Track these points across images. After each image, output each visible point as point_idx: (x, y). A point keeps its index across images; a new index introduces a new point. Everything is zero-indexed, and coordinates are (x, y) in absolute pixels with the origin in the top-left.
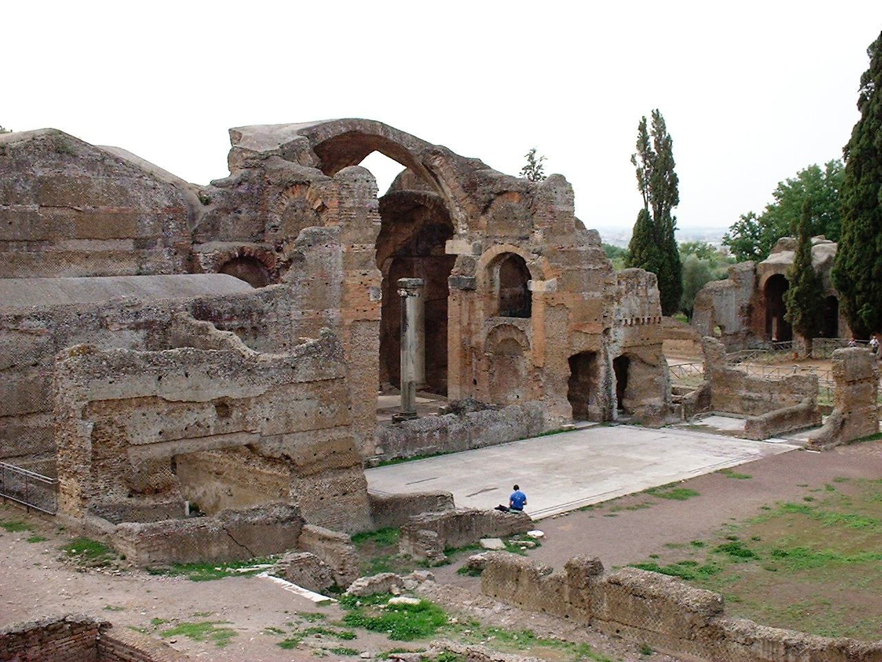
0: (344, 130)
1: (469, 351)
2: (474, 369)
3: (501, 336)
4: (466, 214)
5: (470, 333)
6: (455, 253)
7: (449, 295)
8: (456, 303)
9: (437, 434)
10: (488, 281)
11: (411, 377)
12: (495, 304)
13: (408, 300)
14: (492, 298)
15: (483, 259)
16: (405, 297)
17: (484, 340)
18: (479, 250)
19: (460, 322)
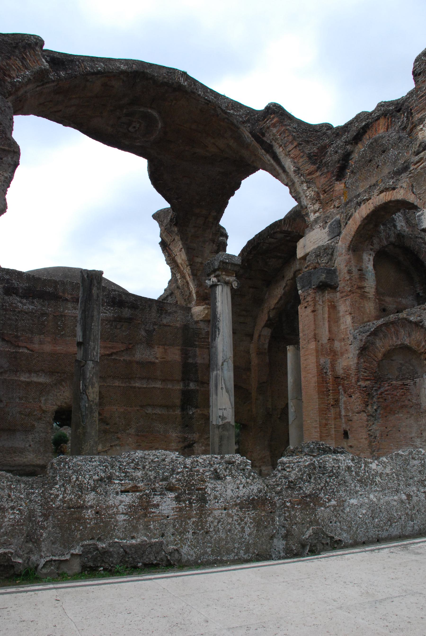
0: (123, 67)
1: (332, 385)
2: (343, 413)
3: (382, 346)
4: (317, 190)
5: (334, 354)
6: (308, 251)
7: (299, 303)
8: (309, 310)
9: (167, 505)
10: (354, 269)
11: (223, 418)
12: (370, 307)
13: (219, 289)
14: (363, 296)
15: (344, 238)
16: (214, 286)
17: (356, 361)
18: (336, 231)
19: (316, 338)
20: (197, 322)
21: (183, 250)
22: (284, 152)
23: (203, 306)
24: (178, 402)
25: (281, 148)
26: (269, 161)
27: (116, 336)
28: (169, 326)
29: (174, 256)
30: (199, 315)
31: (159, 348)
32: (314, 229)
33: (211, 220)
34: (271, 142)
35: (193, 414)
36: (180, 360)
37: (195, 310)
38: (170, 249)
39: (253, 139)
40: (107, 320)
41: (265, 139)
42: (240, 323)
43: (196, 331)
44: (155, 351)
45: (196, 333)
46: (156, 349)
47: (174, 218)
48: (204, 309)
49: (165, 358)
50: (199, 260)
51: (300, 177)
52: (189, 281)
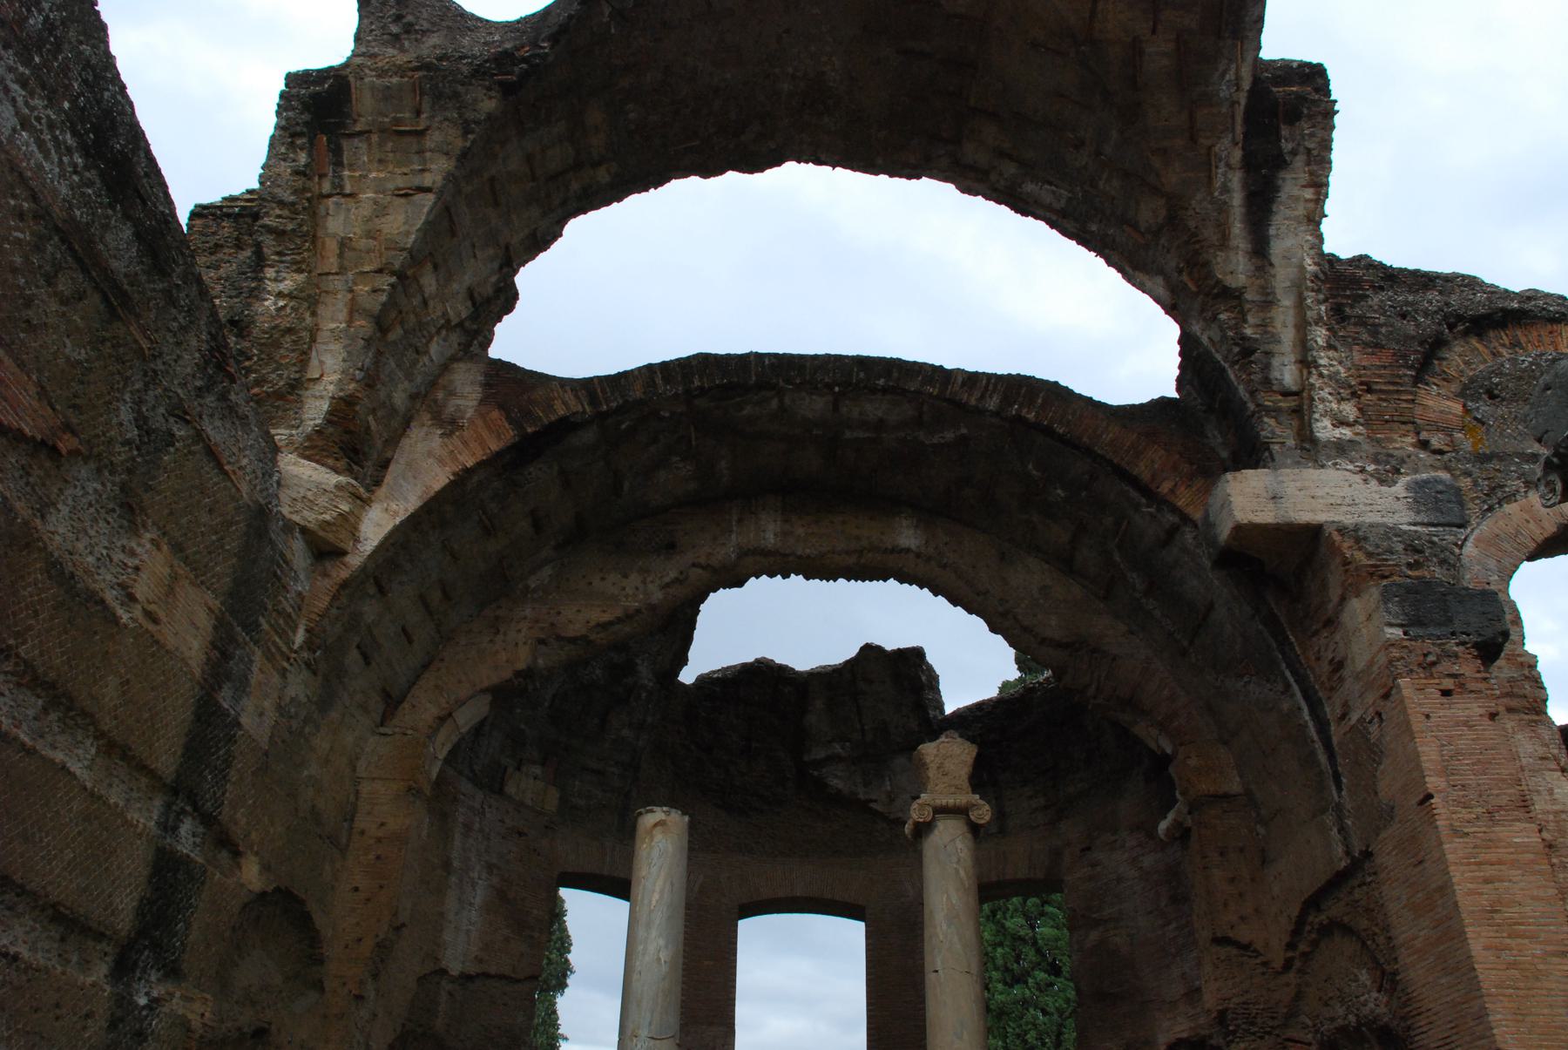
20: (289, 527)
21: (429, 200)
22: (1311, 205)
23: (336, 471)
24: (122, 906)
25: (1311, 190)
26: (1226, 189)
27: (30, 326)
28: (219, 466)
29: (326, 187)
30: (310, 504)
31: (159, 548)
32: (1323, 466)
33: (575, 186)
34: (1294, 153)
35: (148, 1007)
36: (197, 672)
37: (294, 470)
38: (337, 152)
39: (1243, 102)
40: (34, 197)
41: (1285, 131)
42: (404, 630)
43: (279, 566)
44: (133, 554)
45: (275, 575)
46: (143, 545)
47: (524, 60)
48: (338, 487)
49: (156, 621)
50: (429, 282)
51: (1320, 302)
52: (323, 336)
